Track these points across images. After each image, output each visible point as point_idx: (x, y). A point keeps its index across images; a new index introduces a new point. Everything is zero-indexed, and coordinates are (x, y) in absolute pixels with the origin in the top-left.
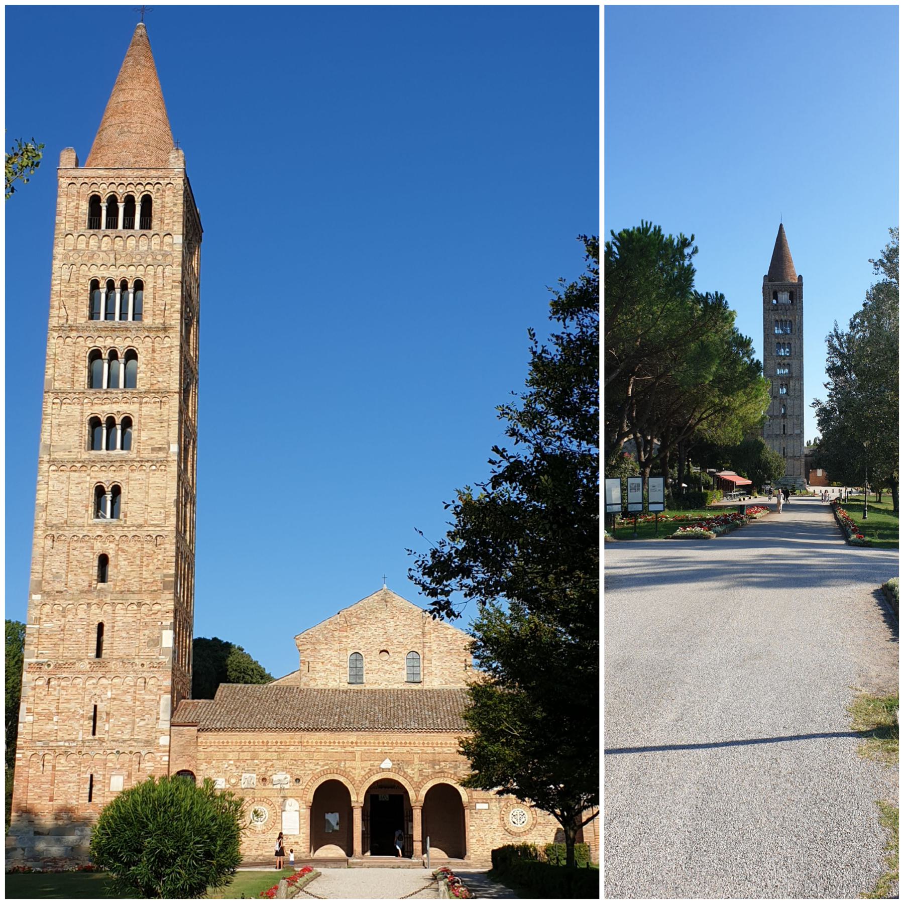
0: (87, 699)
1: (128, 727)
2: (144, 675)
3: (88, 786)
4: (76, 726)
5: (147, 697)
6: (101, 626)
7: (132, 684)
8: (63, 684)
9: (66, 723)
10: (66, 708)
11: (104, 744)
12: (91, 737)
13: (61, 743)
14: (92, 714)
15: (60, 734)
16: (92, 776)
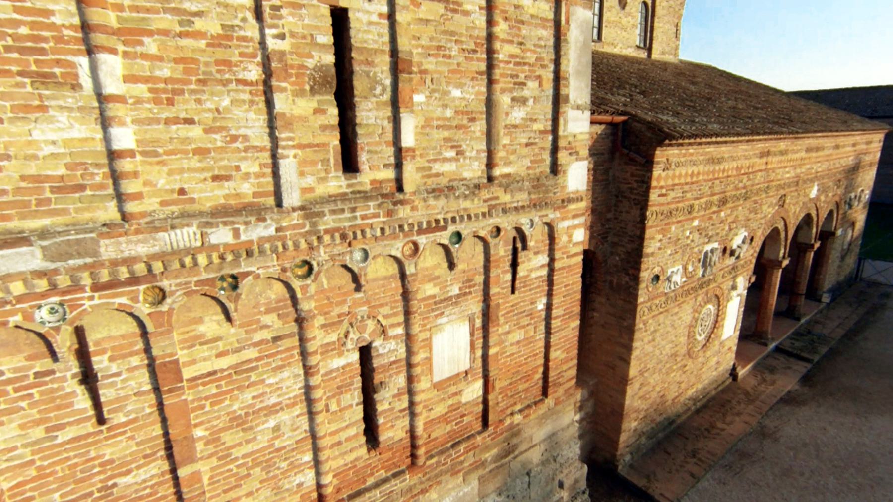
3: (355, 397)
9: (185, 107)
11: (403, 212)
12: (338, 183)
13: (186, 236)
14: (330, 59)
16: (365, 353)
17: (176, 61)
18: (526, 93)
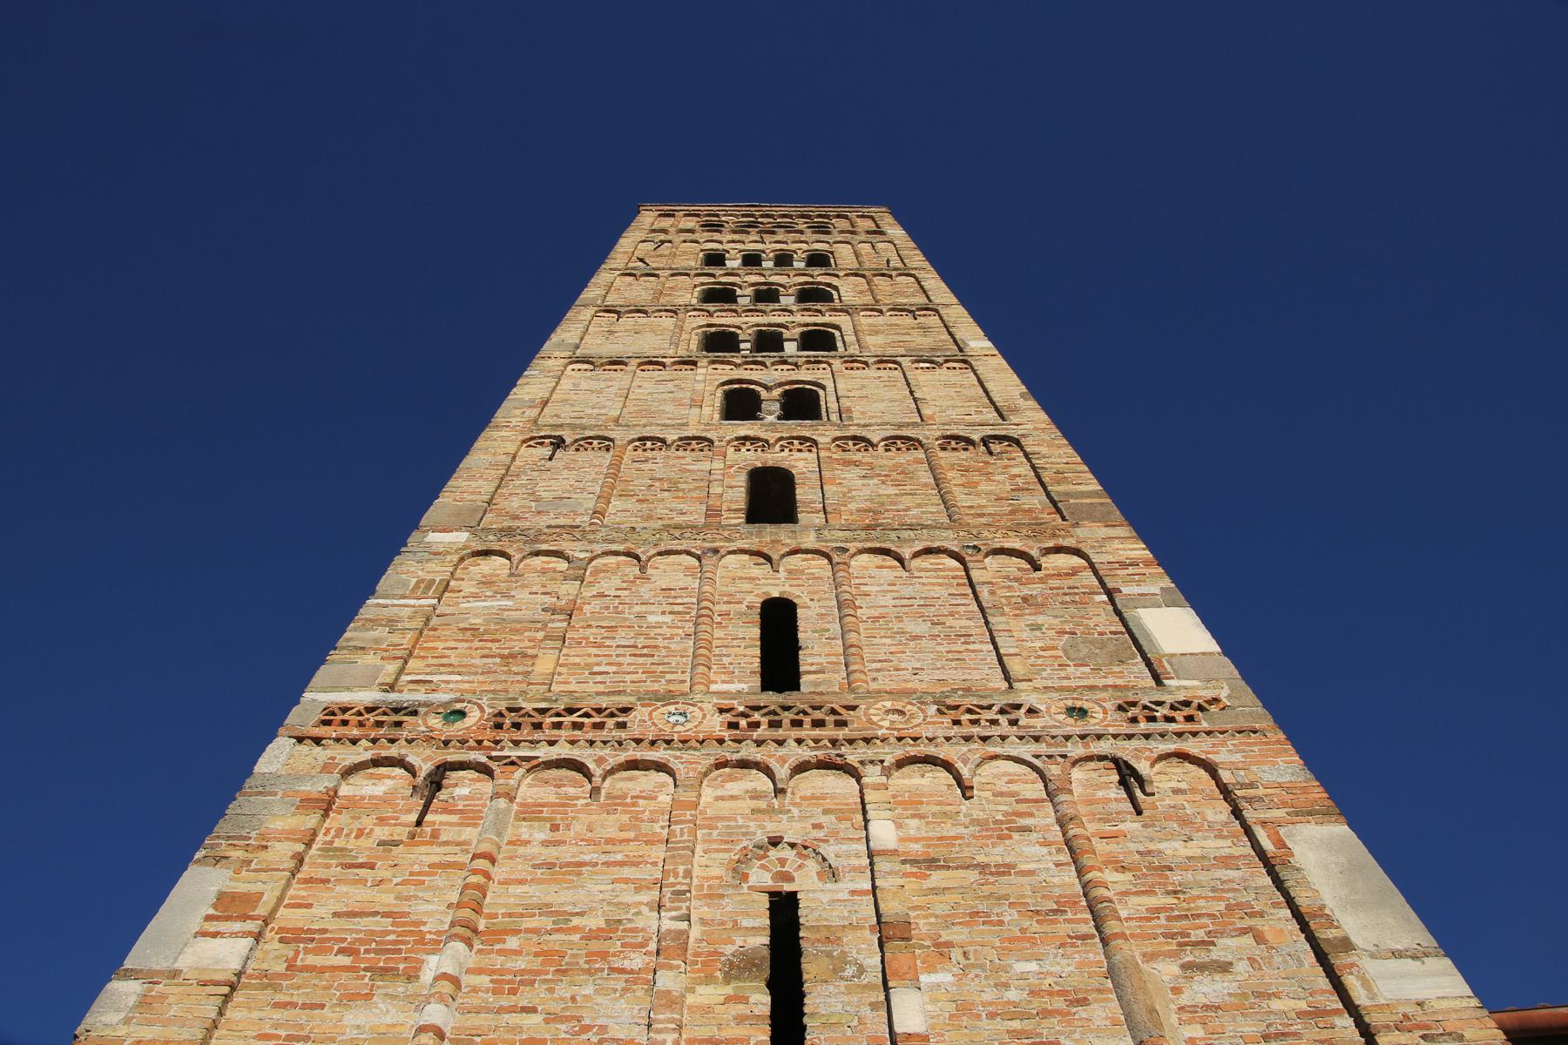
0: (709, 865)
9: (524, 998)
10: (544, 909)
17: (536, 955)
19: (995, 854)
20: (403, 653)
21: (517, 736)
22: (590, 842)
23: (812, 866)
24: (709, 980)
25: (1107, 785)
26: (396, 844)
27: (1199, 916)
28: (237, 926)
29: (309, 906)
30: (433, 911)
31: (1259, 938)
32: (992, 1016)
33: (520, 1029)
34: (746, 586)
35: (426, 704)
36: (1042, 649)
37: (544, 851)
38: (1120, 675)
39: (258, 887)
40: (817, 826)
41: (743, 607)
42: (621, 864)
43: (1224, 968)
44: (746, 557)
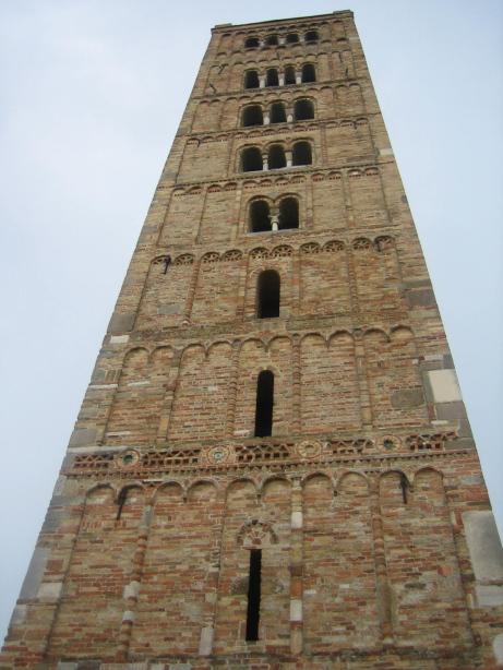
1: (368, 609)
2: (395, 466)
4: (192, 610)
5: (416, 522)
6: (266, 382)
7: (362, 490)
8: (163, 500)
9: (160, 604)
10: (166, 561)
12: (241, 646)
14: (246, 575)
15: (139, 638)
18: (421, 580)
19: (341, 527)
20: (104, 421)
21: (153, 469)
22: (184, 526)
23: (269, 535)
24: (226, 594)
25: (394, 487)
26: (110, 529)
27: (417, 560)
28: (56, 577)
29: (80, 563)
30: (126, 564)
31: (440, 571)
32: (328, 610)
33: (158, 619)
34: (252, 363)
35: (117, 452)
36: (382, 400)
37: (168, 531)
38: (413, 416)
39: (62, 557)
40: (272, 514)
41: (250, 378)
42: (195, 537)
43: (422, 587)
44: (253, 343)
